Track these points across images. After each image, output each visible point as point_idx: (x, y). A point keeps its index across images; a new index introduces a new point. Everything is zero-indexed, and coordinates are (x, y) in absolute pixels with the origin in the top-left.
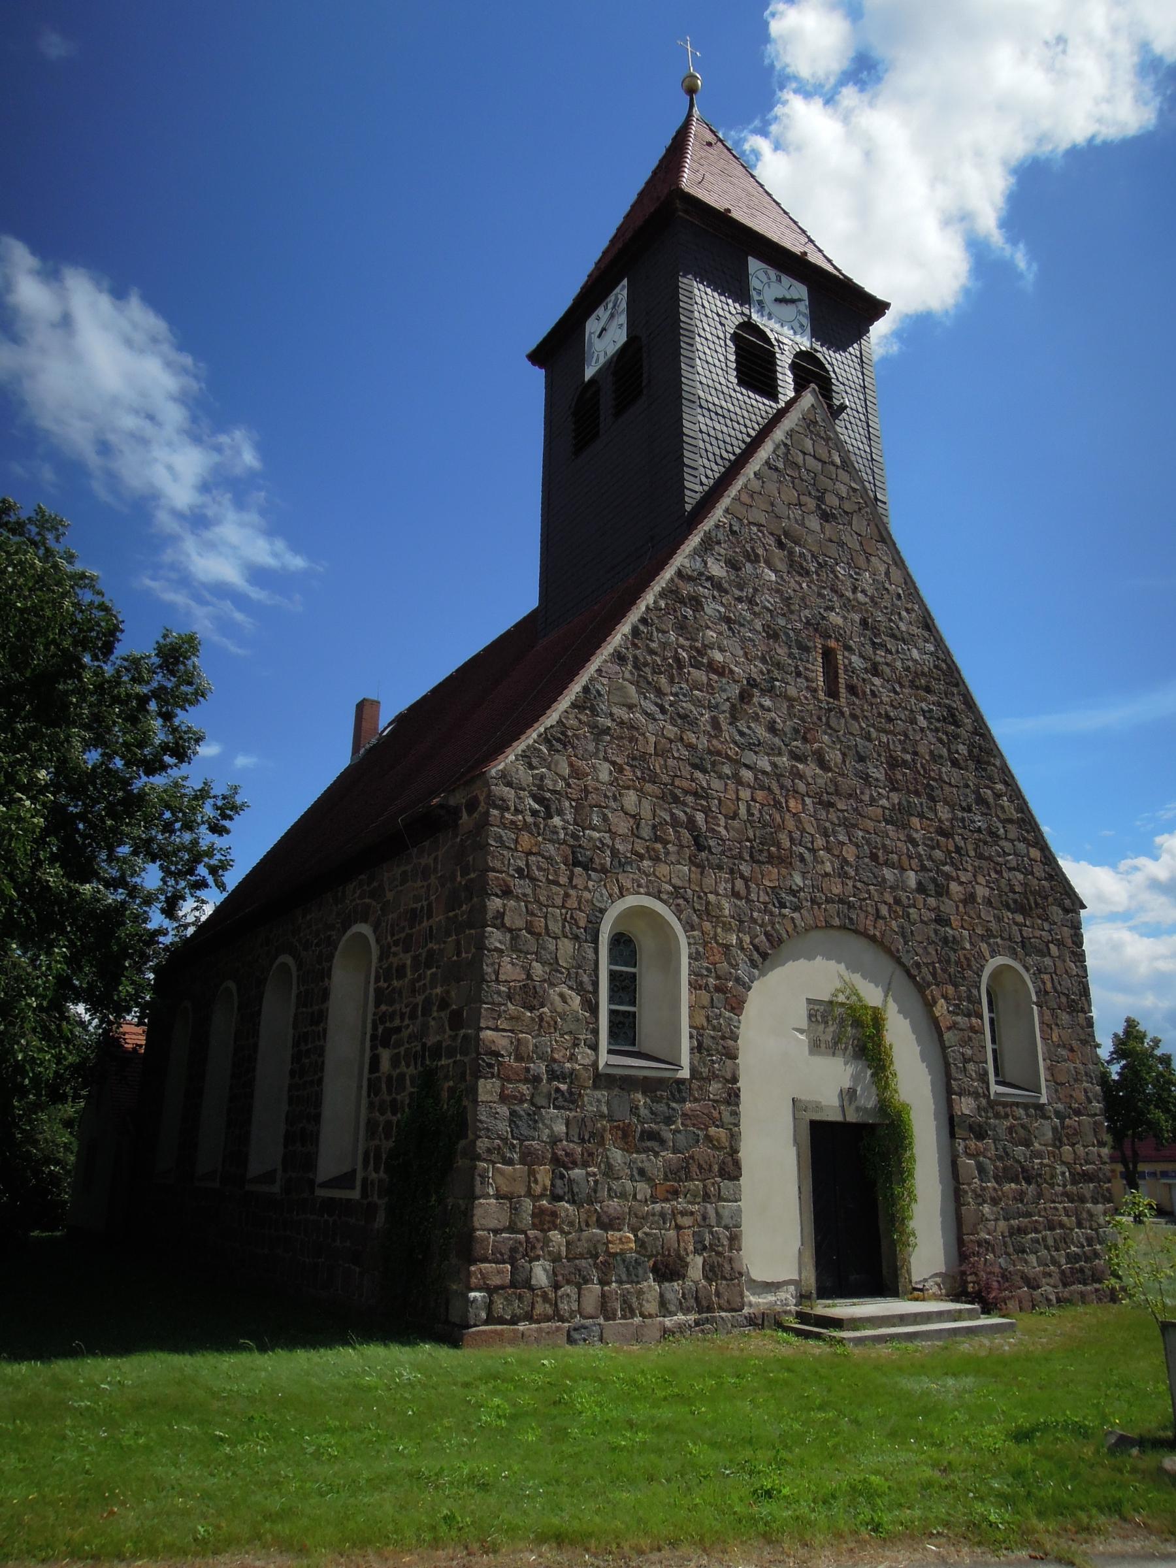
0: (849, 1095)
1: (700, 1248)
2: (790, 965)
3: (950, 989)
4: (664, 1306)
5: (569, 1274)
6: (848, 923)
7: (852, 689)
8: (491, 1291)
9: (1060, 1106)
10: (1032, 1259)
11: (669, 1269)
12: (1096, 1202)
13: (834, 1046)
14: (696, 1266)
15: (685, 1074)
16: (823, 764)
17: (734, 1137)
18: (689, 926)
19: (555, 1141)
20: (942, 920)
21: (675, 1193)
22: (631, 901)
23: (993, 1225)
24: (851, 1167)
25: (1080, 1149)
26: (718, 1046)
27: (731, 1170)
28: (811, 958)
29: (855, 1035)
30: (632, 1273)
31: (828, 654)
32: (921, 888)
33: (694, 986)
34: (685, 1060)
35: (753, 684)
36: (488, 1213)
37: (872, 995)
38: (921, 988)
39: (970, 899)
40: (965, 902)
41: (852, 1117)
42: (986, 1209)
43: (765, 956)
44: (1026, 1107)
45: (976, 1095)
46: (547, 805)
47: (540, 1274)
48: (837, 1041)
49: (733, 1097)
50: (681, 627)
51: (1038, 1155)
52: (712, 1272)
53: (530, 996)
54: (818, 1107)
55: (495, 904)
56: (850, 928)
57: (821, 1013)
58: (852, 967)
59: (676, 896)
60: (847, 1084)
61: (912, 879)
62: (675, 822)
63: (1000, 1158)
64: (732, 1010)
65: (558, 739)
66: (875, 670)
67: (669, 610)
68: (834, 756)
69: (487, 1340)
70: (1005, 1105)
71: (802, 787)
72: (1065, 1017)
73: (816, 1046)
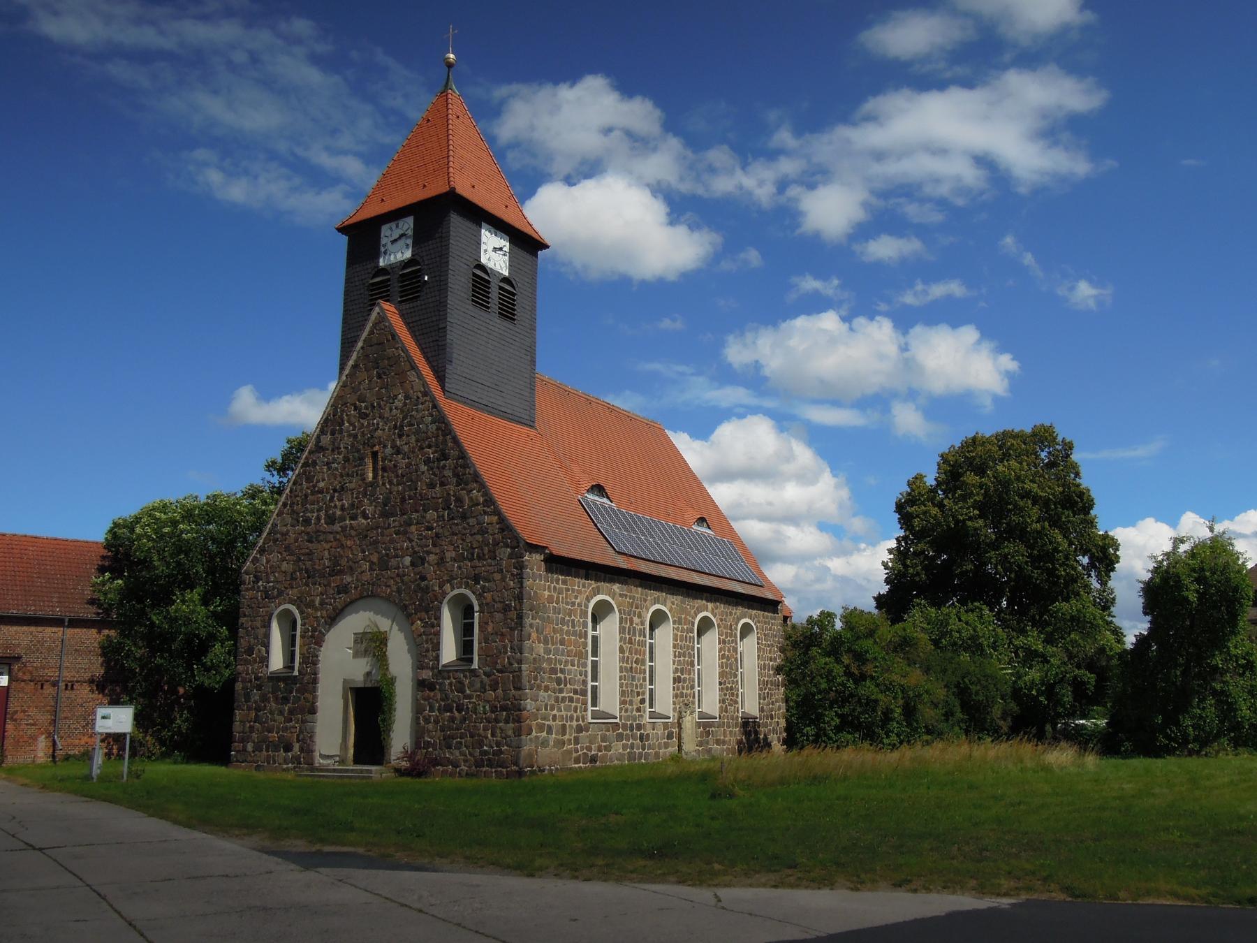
0: (368, 674)
1: (298, 741)
2: (348, 618)
3: (423, 615)
4: (286, 762)
5: (258, 748)
6: (366, 596)
7: (384, 469)
8: (237, 752)
9: (487, 669)
10: (457, 752)
11: (288, 748)
12: (507, 722)
13: (366, 653)
14: (296, 747)
15: (296, 673)
16: (365, 516)
17: (315, 697)
18: (301, 613)
19: (256, 702)
20: (423, 578)
21: (291, 720)
22: (282, 607)
23: (434, 736)
24: (369, 704)
25: (500, 691)
26: (311, 660)
27: (313, 711)
28: (357, 612)
29: (373, 645)
30: (276, 749)
31: (375, 455)
32: (412, 564)
33: (302, 637)
34: (296, 668)
35: (335, 490)
36: (237, 726)
37: (384, 624)
38: (409, 616)
39: (442, 560)
40: (438, 564)
41: (369, 685)
42: (430, 726)
43: (333, 619)
44: (463, 671)
45: (432, 669)
46: (257, 579)
47: (250, 747)
48: (366, 651)
49: (315, 681)
50: (309, 480)
51: (469, 697)
52: (302, 750)
53: (250, 651)
54: (353, 681)
55: (242, 620)
56: (374, 596)
57: (360, 638)
58: (376, 613)
59: (298, 602)
60: (368, 669)
61: (407, 560)
62: (300, 570)
63: (442, 700)
64: (316, 644)
65: (262, 551)
66: (398, 452)
67: (305, 472)
68: (369, 510)
69: (237, 767)
70: (449, 672)
71: (353, 533)
72: (498, 616)
73: (356, 655)
